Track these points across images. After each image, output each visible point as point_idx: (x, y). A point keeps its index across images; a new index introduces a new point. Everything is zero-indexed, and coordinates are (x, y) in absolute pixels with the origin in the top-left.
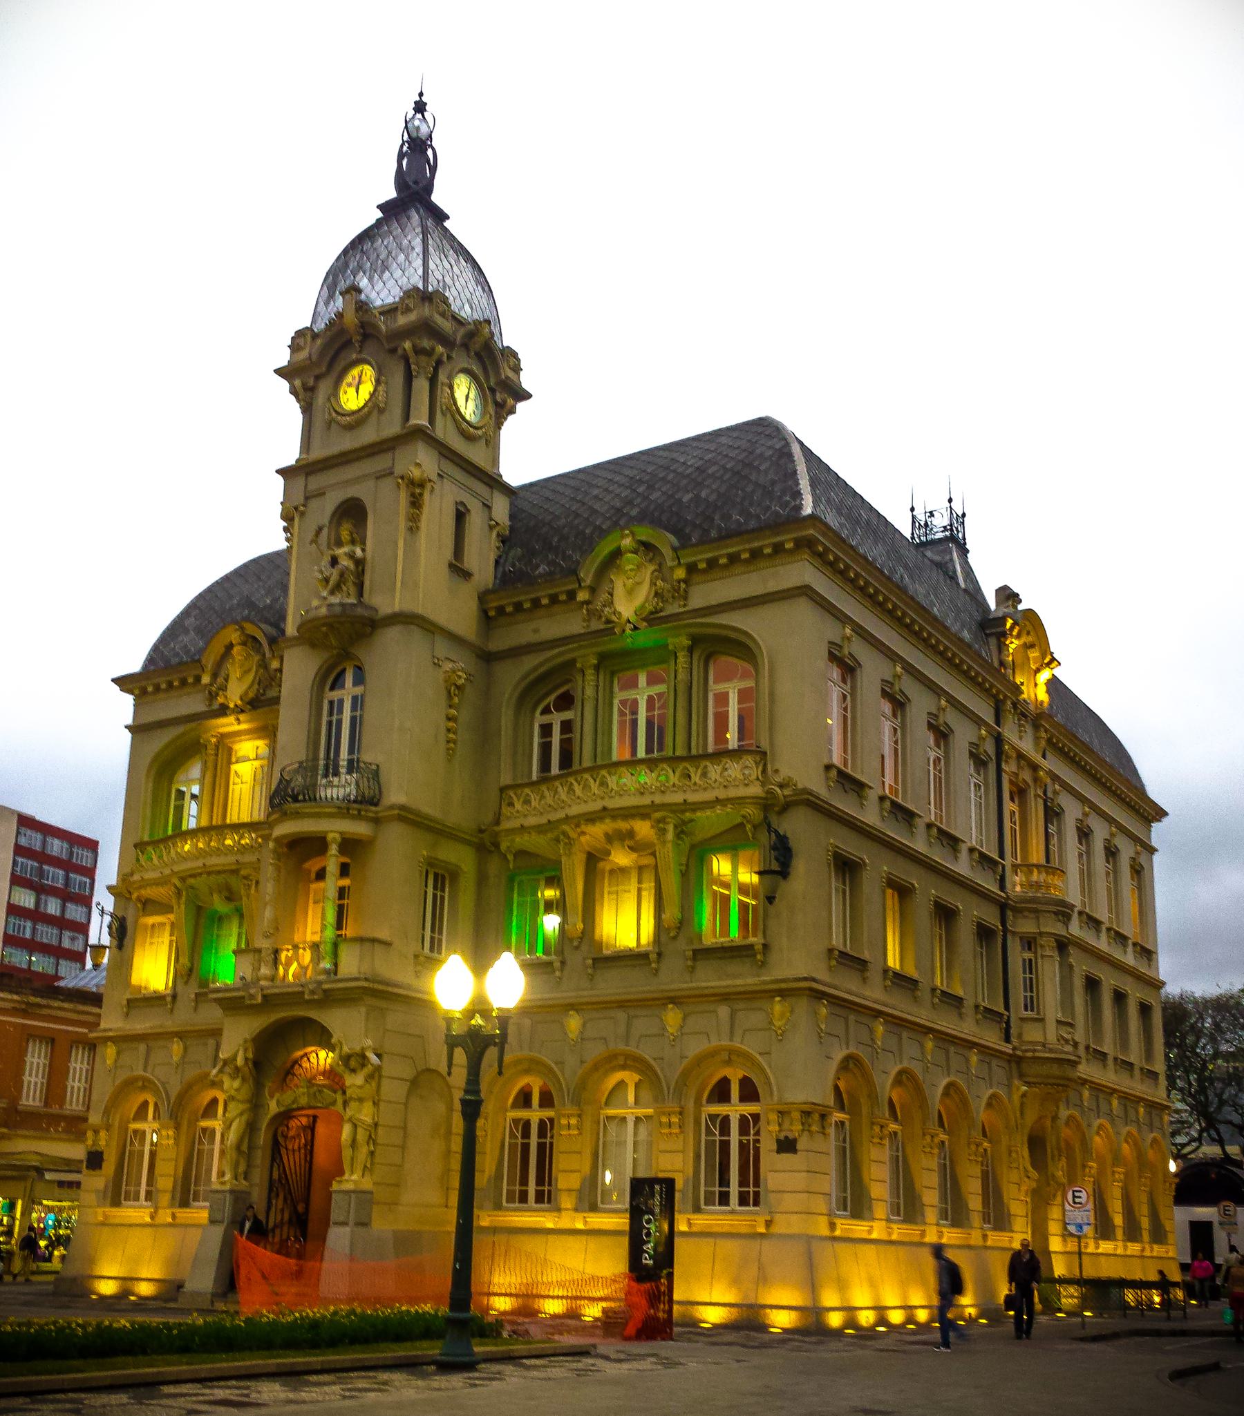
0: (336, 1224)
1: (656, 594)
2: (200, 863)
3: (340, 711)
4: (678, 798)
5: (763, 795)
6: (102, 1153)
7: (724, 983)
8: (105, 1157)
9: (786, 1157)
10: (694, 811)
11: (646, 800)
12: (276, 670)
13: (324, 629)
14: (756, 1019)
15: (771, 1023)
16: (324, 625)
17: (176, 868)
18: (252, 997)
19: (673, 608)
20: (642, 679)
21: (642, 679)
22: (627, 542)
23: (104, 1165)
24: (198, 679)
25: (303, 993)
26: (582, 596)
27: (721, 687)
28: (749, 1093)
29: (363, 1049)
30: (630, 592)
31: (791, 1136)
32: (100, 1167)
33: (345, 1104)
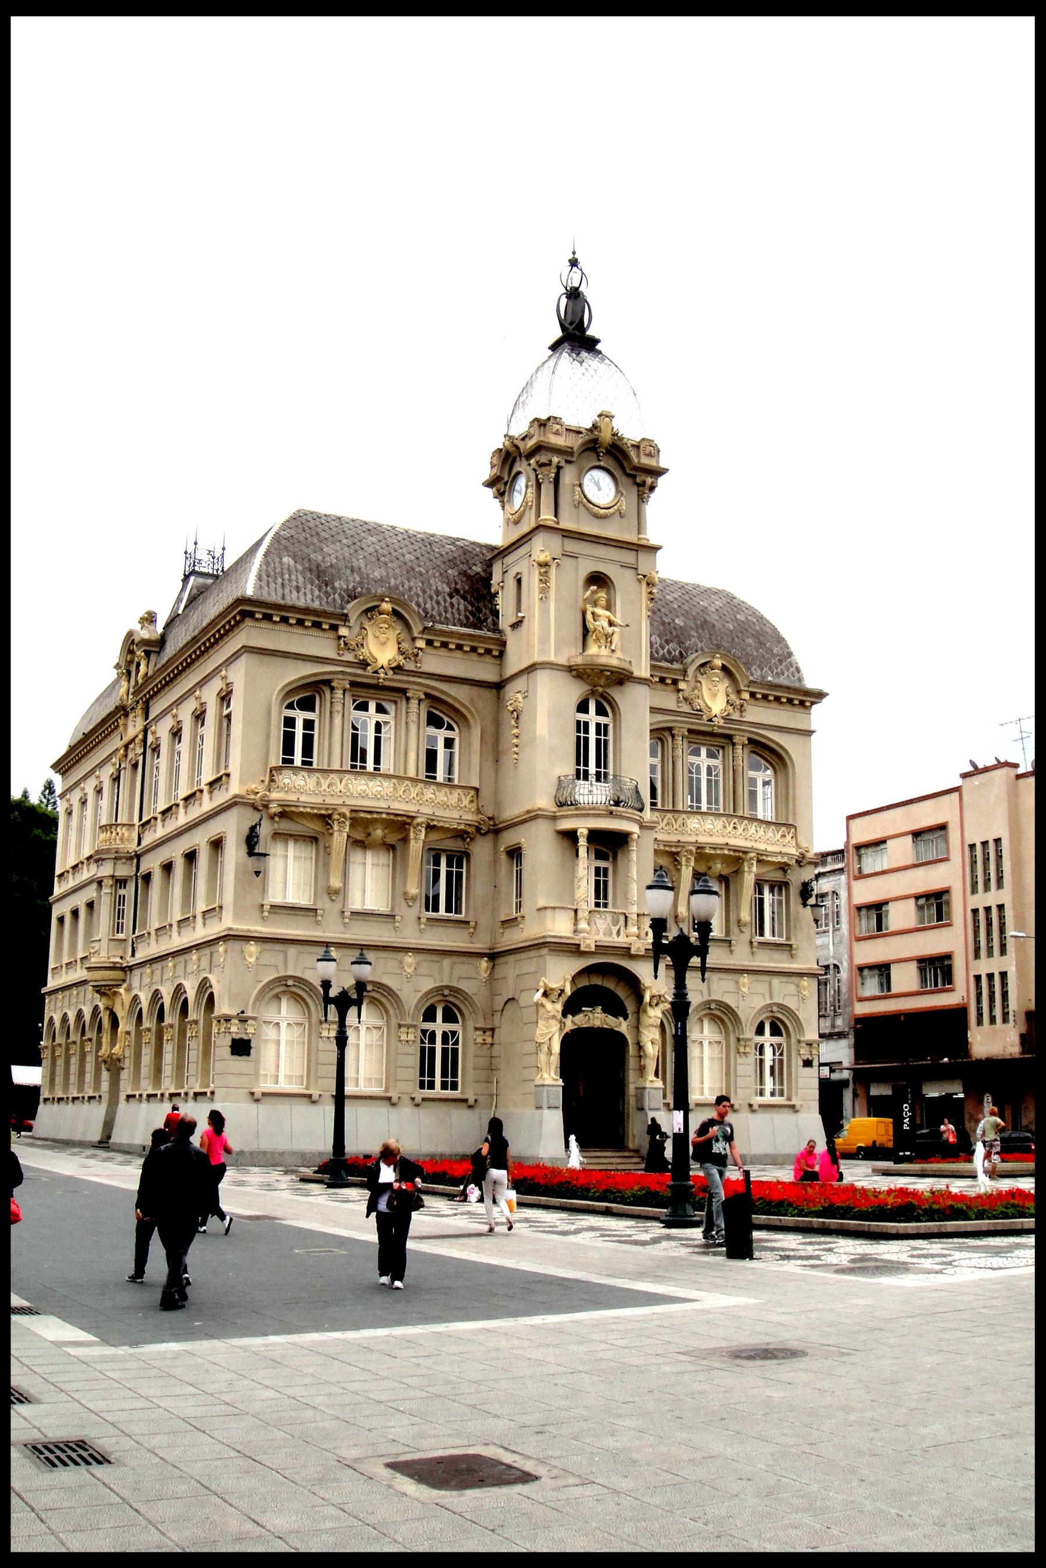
0: (650, 1109)
1: (728, 701)
2: (383, 804)
3: (586, 731)
4: (762, 847)
5: (798, 854)
6: (249, 1041)
7: (773, 965)
8: (252, 1045)
9: (807, 1069)
10: (767, 856)
11: (749, 844)
12: (419, 649)
13: (609, 673)
14: (791, 988)
15: (799, 992)
16: (608, 671)
17: (349, 802)
18: (588, 946)
19: (736, 716)
20: (704, 751)
21: (704, 751)
22: (718, 662)
23: (252, 1051)
24: (334, 628)
25: (629, 949)
26: (682, 685)
27: (752, 774)
28: (776, 1031)
29: (665, 993)
30: (714, 696)
31: (810, 1058)
32: (249, 1054)
33: (637, 1028)
